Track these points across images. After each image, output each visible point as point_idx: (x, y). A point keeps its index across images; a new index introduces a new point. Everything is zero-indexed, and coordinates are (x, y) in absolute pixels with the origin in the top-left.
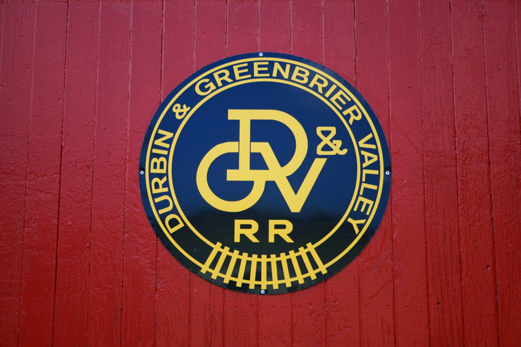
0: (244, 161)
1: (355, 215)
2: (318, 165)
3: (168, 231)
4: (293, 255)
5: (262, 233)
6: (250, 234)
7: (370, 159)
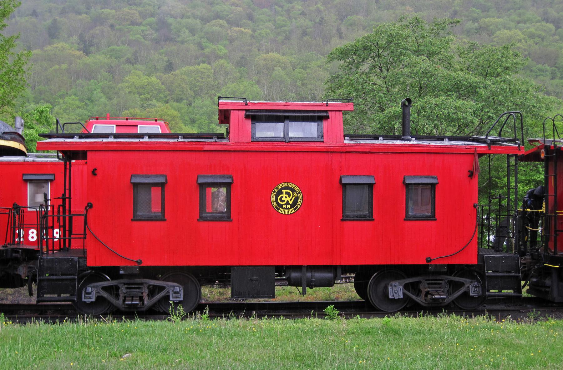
0: (284, 197)
1: (299, 204)
2: (294, 198)
3: (274, 206)
4: (290, 210)
5: (286, 207)
6: (285, 207)
7: (300, 197)
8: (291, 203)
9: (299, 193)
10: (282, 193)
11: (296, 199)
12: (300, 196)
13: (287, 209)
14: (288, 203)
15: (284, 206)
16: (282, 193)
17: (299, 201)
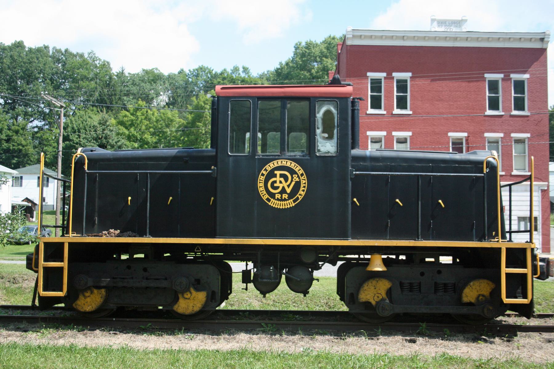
0: (278, 182)
1: (300, 195)
5: (281, 197)
7: (304, 182)
8: (289, 190)
9: (302, 175)
10: (275, 176)
11: (298, 184)
12: (304, 181)
13: (282, 200)
14: (283, 191)
15: (278, 196)
16: (275, 176)
17: (302, 189)
